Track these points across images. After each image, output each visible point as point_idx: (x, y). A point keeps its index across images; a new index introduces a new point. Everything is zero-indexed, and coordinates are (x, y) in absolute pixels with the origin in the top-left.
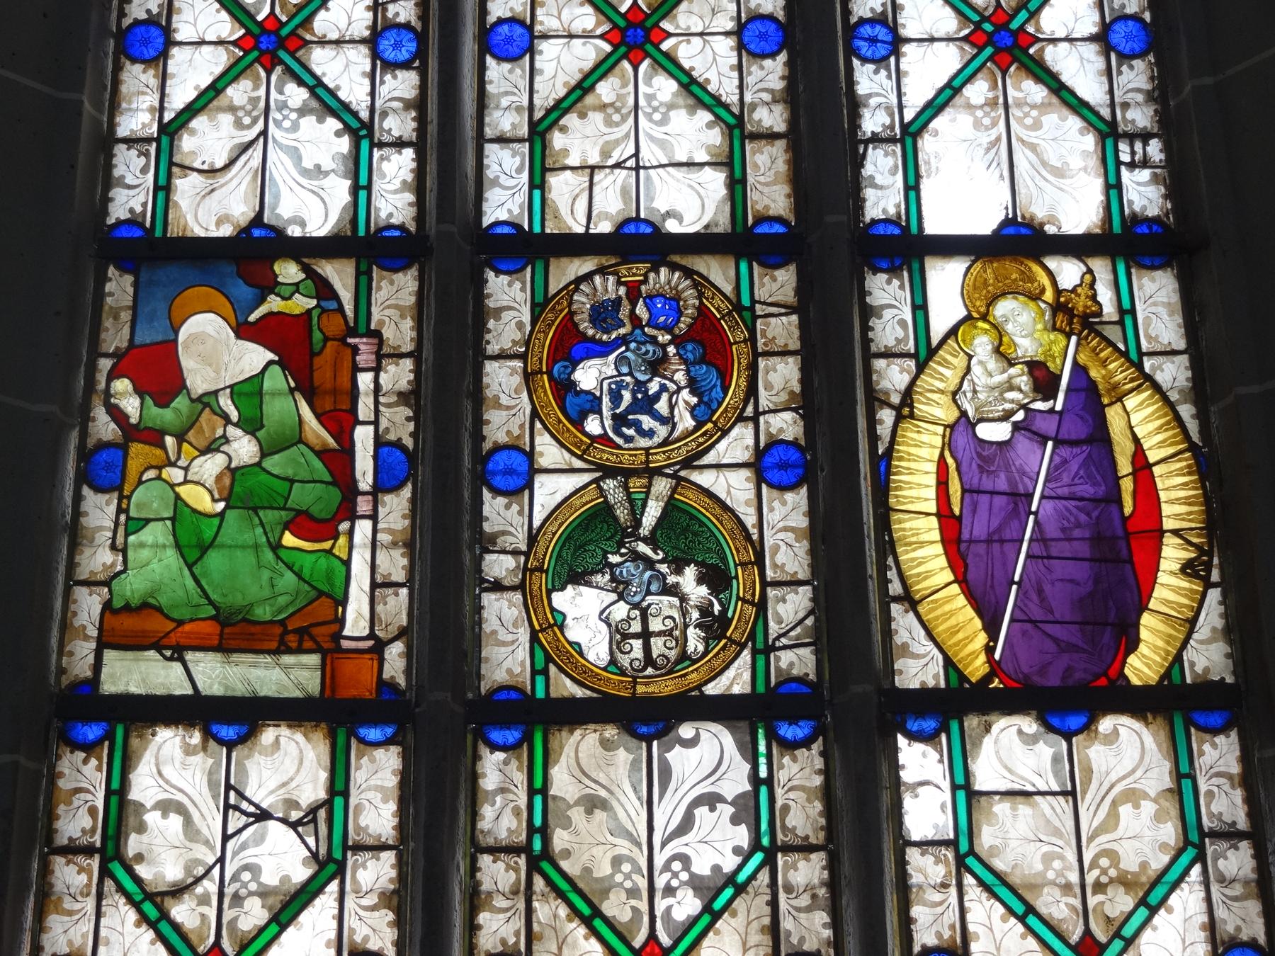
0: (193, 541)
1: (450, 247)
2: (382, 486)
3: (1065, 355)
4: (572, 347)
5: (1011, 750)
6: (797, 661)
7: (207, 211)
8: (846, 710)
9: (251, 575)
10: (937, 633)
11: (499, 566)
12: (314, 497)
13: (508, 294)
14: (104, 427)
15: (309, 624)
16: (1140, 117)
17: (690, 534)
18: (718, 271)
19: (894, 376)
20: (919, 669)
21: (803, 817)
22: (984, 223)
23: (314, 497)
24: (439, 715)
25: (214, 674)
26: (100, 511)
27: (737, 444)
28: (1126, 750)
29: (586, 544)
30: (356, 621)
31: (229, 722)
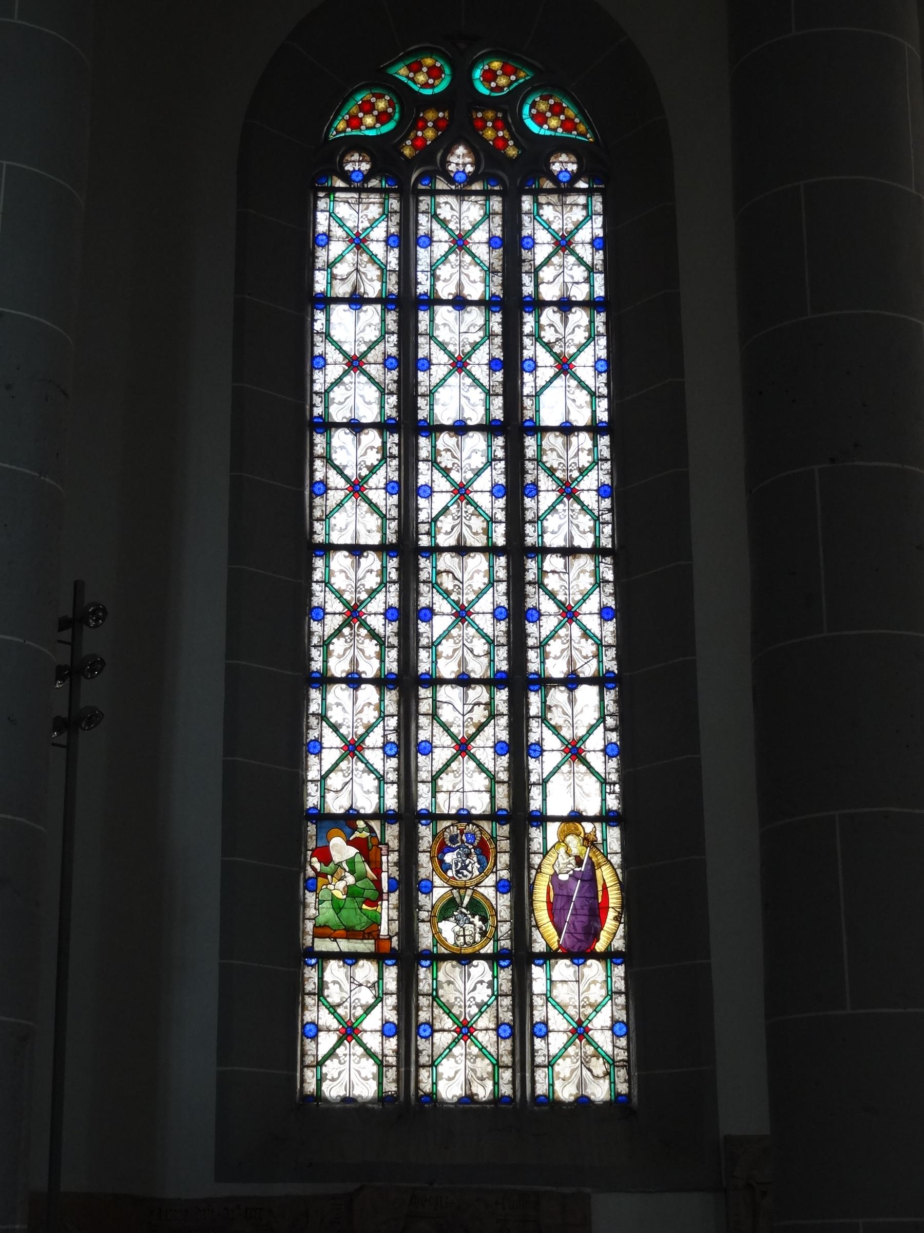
0: (338, 907)
1: (407, 816)
2: (391, 891)
3: (586, 854)
4: (443, 849)
5: (563, 969)
6: (506, 944)
7: (336, 805)
8: (519, 958)
9: (355, 917)
10: (545, 935)
11: (424, 915)
12: (370, 894)
13: (425, 832)
14: (310, 873)
15: (371, 931)
16: (614, 777)
17: (477, 907)
18: (486, 825)
19: (536, 860)
20: (539, 947)
21: (506, 987)
22: (565, 813)
23: (370, 894)
24: (407, 957)
25: (345, 945)
26: (311, 898)
27: (491, 880)
28: (594, 969)
29: (448, 909)
30: (384, 931)
31: (349, 959)
